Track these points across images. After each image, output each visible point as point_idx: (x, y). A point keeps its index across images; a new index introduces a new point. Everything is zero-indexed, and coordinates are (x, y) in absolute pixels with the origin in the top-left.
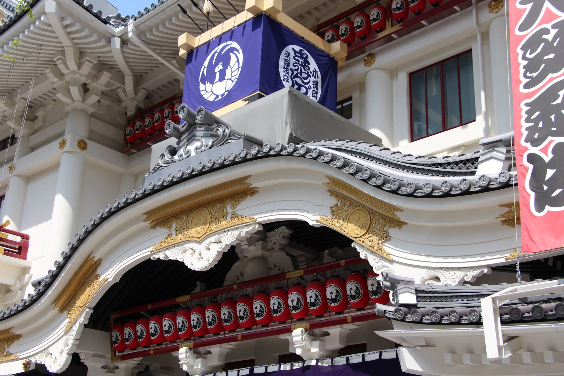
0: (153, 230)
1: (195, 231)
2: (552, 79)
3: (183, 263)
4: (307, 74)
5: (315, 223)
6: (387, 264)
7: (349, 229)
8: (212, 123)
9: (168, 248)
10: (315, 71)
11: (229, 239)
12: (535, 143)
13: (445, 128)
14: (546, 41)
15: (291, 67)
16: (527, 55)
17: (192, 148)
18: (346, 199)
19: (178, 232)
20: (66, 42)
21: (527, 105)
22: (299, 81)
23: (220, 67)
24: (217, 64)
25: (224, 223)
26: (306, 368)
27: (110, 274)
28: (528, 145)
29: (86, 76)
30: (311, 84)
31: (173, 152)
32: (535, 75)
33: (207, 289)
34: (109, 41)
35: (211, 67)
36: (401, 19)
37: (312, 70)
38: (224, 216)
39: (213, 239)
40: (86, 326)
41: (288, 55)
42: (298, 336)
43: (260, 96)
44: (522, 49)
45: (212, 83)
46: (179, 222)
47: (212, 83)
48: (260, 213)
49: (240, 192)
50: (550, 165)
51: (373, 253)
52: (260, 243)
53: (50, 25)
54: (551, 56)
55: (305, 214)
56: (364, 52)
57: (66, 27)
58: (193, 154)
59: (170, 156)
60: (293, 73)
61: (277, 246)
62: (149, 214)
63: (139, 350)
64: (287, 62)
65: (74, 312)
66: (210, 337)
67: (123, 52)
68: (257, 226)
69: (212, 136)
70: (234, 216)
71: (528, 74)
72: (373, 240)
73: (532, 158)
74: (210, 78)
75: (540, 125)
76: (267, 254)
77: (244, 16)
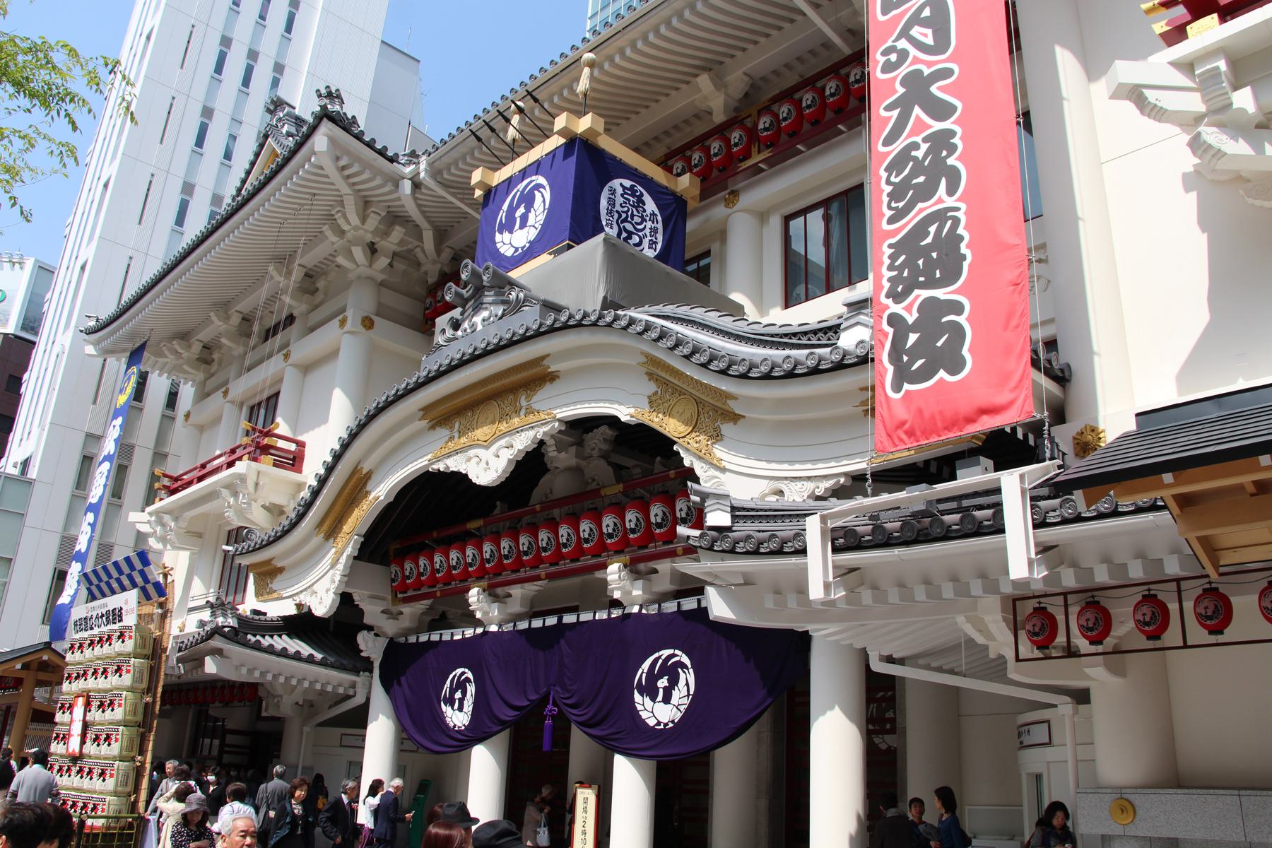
1: (481, 433)
2: (921, 210)
3: (466, 475)
4: (642, 217)
5: (628, 418)
6: (717, 473)
7: (671, 427)
8: (501, 284)
9: (449, 455)
10: (654, 214)
11: (523, 442)
12: (897, 297)
13: (829, 289)
14: (915, 158)
15: (618, 208)
16: (893, 179)
17: (478, 319)
18: (668, 387)
20: (345, 189)
21: (890, 246)
22: (629, 227)
23: (522, 210)
24: (518, 206)
25: (516, 421)
27: (382, 491)
28: (889, 302)
29: (372, 232)
30: (647, 231)
31: (456, 325)
32: (901, 205)
33: (510, 509)
34: (397, 186)
35: (512, 210)
36: (771, 143)
37: (649, 212)
38: (517, 412)
39: (503, 442)
40: (355, 558)
41: (613, 192)
42: (614, 572)
43: (570, 247)
44: (886, 170)
45: (511, 232)
46: (463, 421)
47: (511, 232)
48: (560, 407)
49: (535, 378)
50: (914, 328)
51: (700, 458)
52: (573, 449)
53: (322, 168)
54: (921, 179)
55: (616, 406)
56: (726, 188)
57: (343, 168)
58: (480, 327)
59: (452, 332)
60: (620, 216)
61: (596, 453)
62: (426, 410)
63: (425, 590)
64: (611, 202)
65: (341, 539)
66: (507, 576)
67: (415, 199)
68: (557, 424)
69: (503, 302)
70: (530, 411)
71: (893, 205)
72: (699, 441)
73: (894, 320)
74: (509, 226)
75: (905, 274)
76: (583, 463)
77: (555, 142)
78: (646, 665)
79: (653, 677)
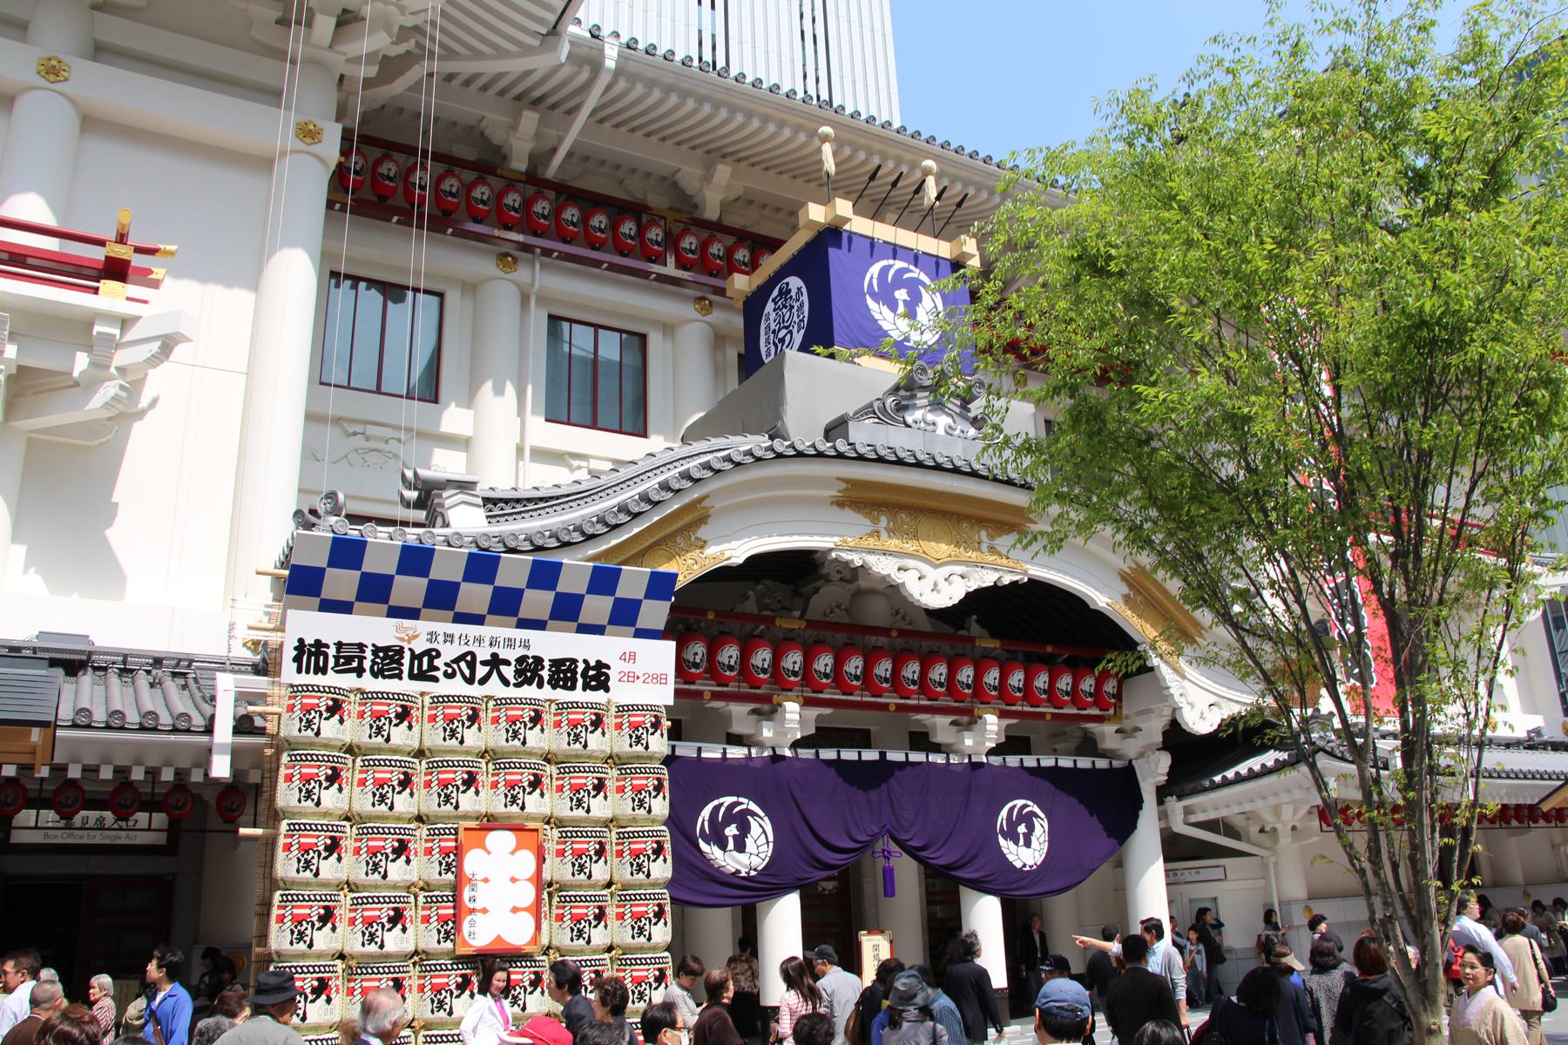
0: (836, 509)
9: (871, 552)
19: (891, 532)
26: (976, 766)
39: (960, 569)
58: (940, 431)
70: (992, 550)
78: (1004, 813)
79: (1012, 825)
